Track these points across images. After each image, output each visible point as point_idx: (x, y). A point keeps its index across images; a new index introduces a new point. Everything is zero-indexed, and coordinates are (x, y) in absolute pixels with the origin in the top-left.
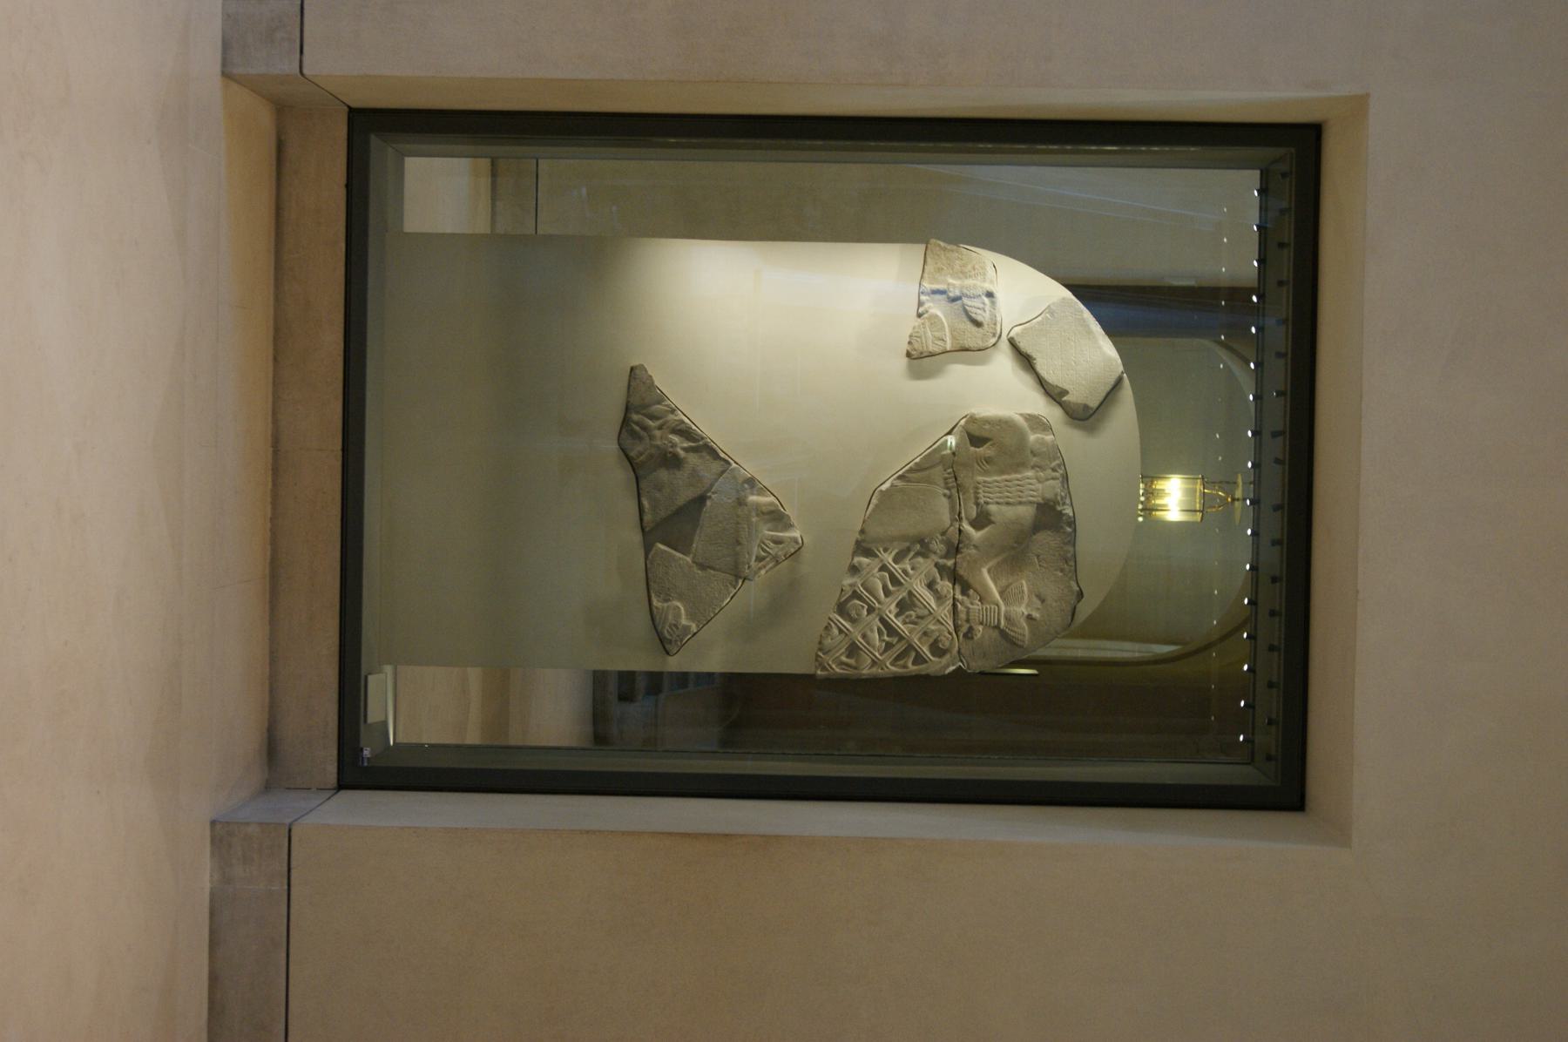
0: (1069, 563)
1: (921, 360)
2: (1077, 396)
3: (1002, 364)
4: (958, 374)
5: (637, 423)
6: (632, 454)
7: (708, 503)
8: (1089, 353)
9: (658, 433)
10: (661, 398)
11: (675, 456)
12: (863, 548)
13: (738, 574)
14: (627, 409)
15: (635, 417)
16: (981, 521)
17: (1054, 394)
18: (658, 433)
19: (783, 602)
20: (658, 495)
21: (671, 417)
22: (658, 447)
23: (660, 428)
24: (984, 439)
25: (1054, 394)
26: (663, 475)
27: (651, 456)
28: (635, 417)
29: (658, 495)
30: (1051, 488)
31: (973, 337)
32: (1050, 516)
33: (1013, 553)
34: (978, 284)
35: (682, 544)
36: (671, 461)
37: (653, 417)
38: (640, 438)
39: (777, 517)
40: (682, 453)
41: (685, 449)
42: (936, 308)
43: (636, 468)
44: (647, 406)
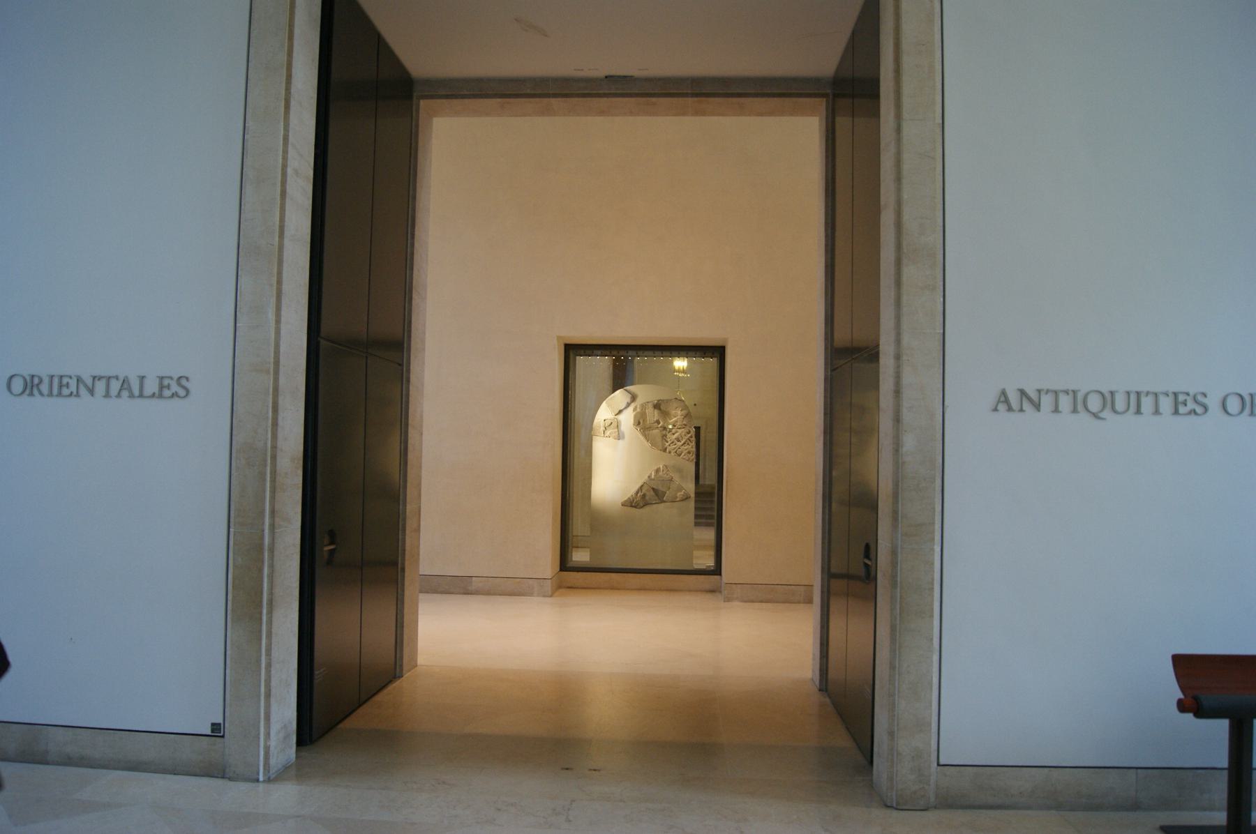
0: (668, 401)
1: (619, 437)
2: (628, 400)
3: (622, 417)
4: (623, 428)
8: (620, 396)
12: (665, 450)
13: (671, 480)
16: (658, 422)
17: (628, 405)
19: (679, 471)
24: (640, 422)
25: (628, 405)
30: (650, 406)
31: (614, 424)
32: (657, 406)
33: (665, 414)
34: (602, 423)
35: (664, 493)
36: (644, 495)
39: (657, 471)
42: (608, 433)
43: (646, 504)
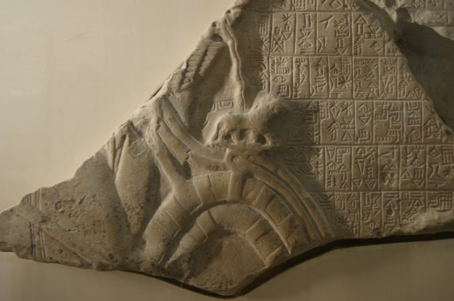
5: (170, 244)
6: (267, 260)
7: (421, 17)
9: (200, 179)
10: (99, 169)
11: (274, 121)
14: (129, 267)
15: (151, 248)
18: (200, 179)
20: (396, 180)
21: (150, 135)
22: (244, 178)
23: (184, 171)
26: (330, 162)
27: (271, 198)
28: (151, 248)
29: (396, 180)
36: (289, 132)
37: (152, 193)
38: (218, 232)
40: (264, 102)
41: (250, 94)
44: (117, 214)
